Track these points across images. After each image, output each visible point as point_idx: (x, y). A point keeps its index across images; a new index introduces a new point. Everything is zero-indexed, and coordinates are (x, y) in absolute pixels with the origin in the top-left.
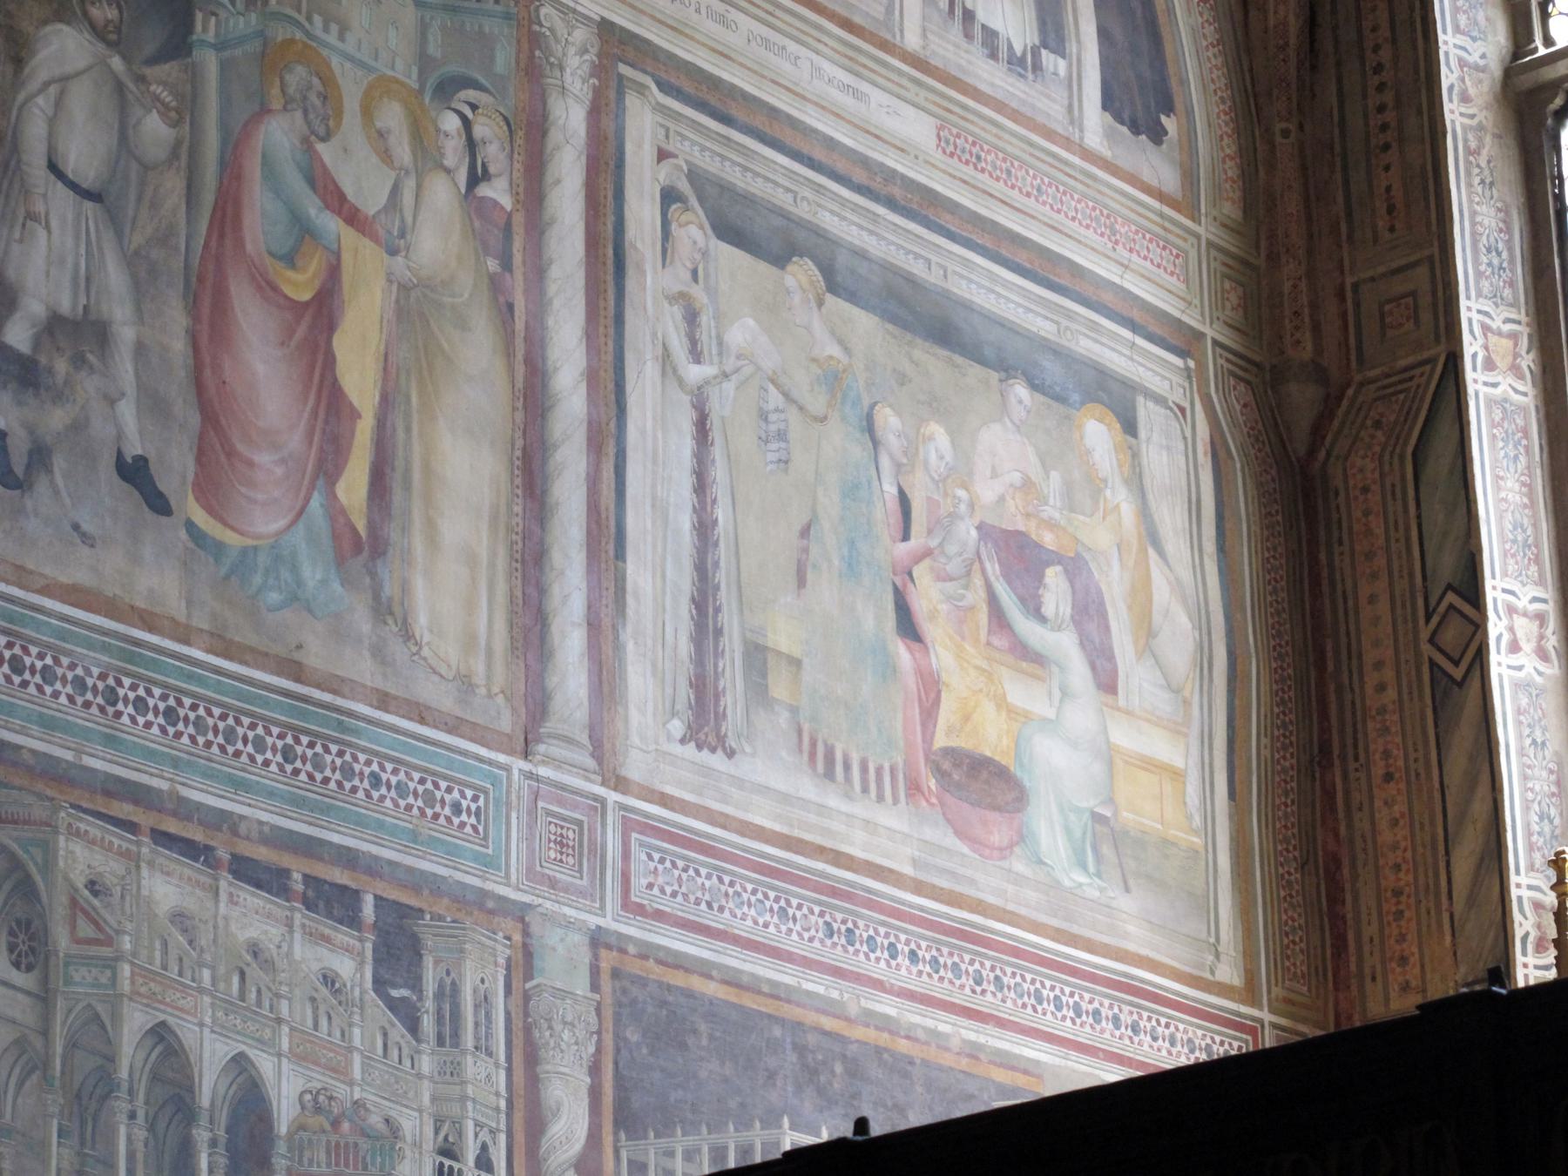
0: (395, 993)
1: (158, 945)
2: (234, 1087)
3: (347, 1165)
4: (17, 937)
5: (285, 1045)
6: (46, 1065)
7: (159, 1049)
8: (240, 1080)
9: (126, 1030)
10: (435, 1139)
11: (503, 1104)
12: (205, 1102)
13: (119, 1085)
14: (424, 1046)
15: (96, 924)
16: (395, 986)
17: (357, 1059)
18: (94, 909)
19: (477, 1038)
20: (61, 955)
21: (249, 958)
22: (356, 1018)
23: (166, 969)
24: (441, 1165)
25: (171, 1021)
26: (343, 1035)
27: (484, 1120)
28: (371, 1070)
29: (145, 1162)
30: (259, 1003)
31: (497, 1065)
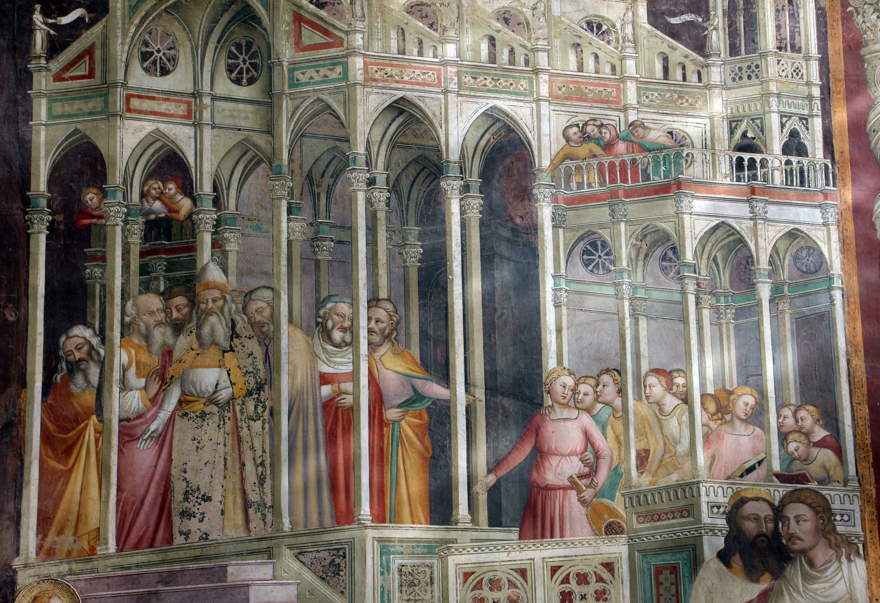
0: (674, 21)
1: (393, 34)
2: (487, 136)
3: (624, 180)
4: (237, 58)
5: (544, 90)
6: (270, 159)
7: (400, 120)
8: (494, 129)
9: (360, 111)
10: (731, 138)
11: (816, 92)
12: (454, 155)
13: (354, 161)
14: (710, 61)
15: (326, 32)
16: (674, 15)
17: (631, 89)
18: (321, 19)
19: (780, 40)
20: (285, 64)
21: (499, 25)
22: (630, 51)
23: (404, 53)
24: (740, 161)
25: (409, 95)
26: (613, 68)
27: (793, 110)
28: (649, 93)
29: (388, 219)
30: (512, 62)
31: (807, 58)
